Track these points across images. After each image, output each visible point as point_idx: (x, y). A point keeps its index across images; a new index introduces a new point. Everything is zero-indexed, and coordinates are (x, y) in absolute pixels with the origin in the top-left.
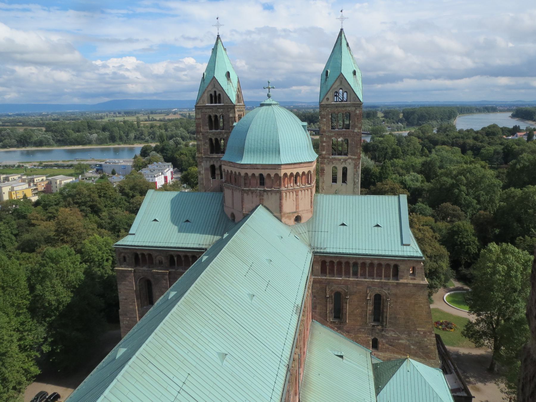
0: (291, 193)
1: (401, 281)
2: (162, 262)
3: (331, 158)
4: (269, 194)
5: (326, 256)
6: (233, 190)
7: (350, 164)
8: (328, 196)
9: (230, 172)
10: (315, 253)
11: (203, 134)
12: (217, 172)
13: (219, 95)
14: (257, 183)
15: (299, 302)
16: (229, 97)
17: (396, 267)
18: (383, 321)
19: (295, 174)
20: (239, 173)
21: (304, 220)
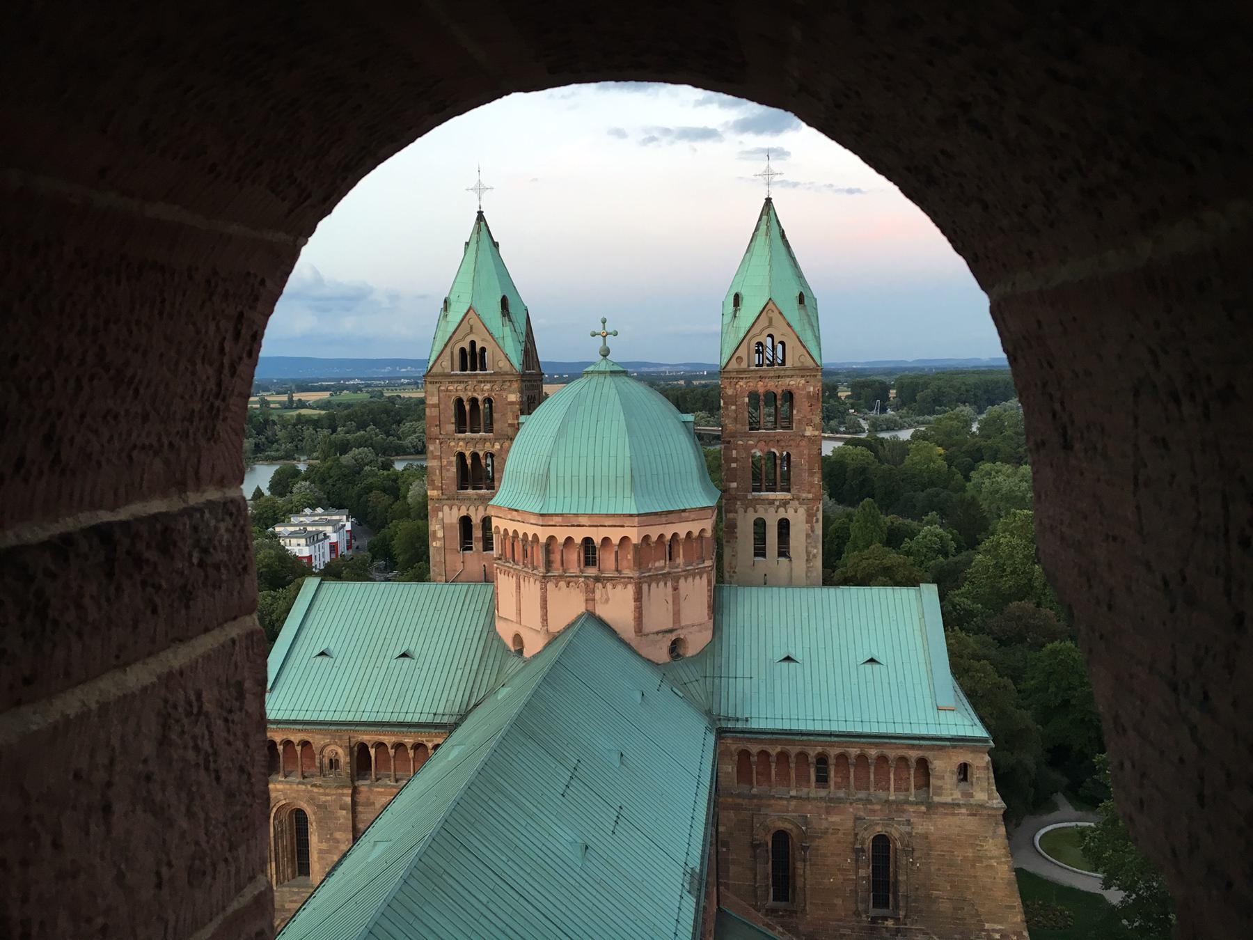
0: (662, 584)
1: (936, 799)
2: (337, 761)
3: (750, 497)
4: (609, 586)
5: (749, 740)
6: (518, 579)
7: (796, 512)
8: (747, 590)
9: (511, 534)
10: (721, 733)
11: (441, 443)
12: (477, 533)
13: (483, 350)
14: (579, 560)
15: (695, 862)
16: (506, 356)
17: (923, 764)
18: (897, 907)
19: (668, 537)
20: (535, 536)
21: (691, 650)
